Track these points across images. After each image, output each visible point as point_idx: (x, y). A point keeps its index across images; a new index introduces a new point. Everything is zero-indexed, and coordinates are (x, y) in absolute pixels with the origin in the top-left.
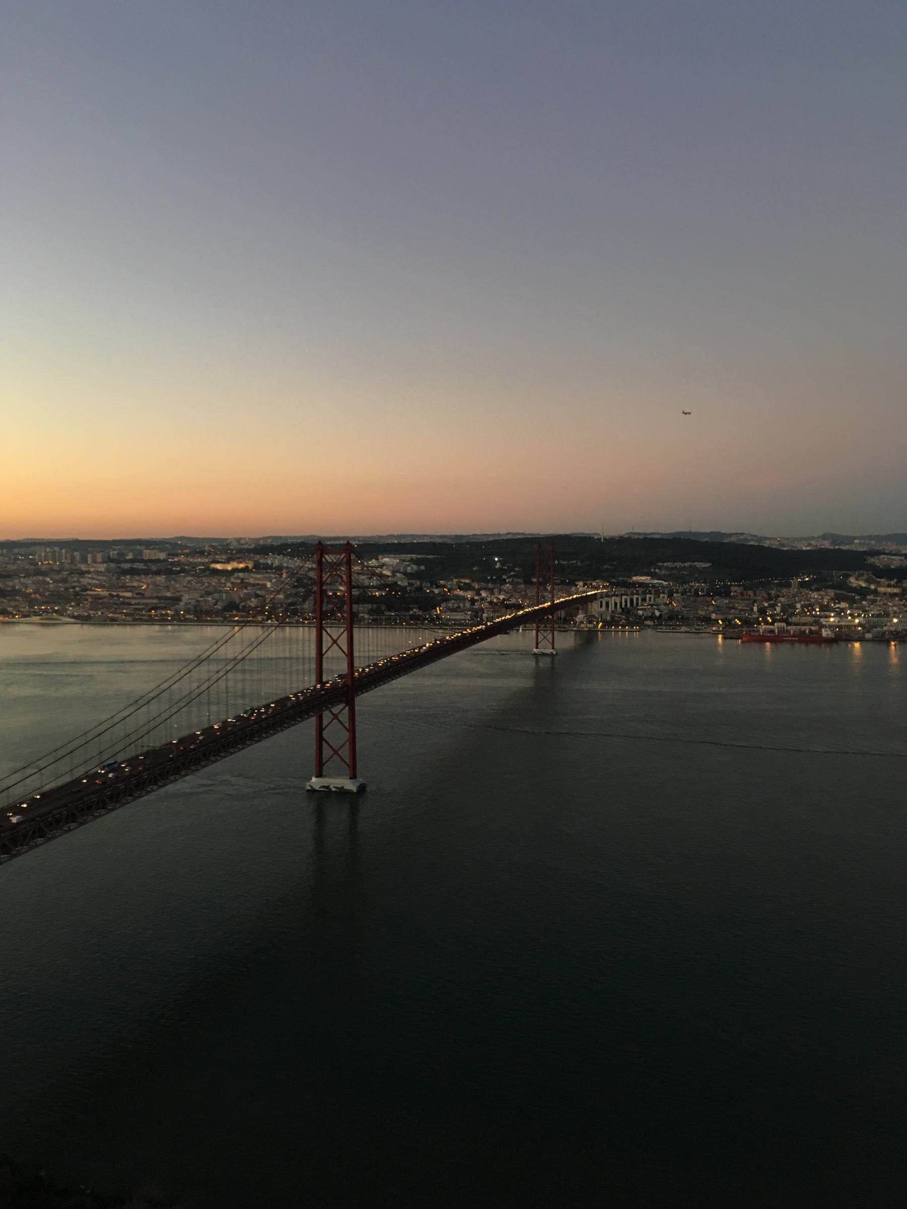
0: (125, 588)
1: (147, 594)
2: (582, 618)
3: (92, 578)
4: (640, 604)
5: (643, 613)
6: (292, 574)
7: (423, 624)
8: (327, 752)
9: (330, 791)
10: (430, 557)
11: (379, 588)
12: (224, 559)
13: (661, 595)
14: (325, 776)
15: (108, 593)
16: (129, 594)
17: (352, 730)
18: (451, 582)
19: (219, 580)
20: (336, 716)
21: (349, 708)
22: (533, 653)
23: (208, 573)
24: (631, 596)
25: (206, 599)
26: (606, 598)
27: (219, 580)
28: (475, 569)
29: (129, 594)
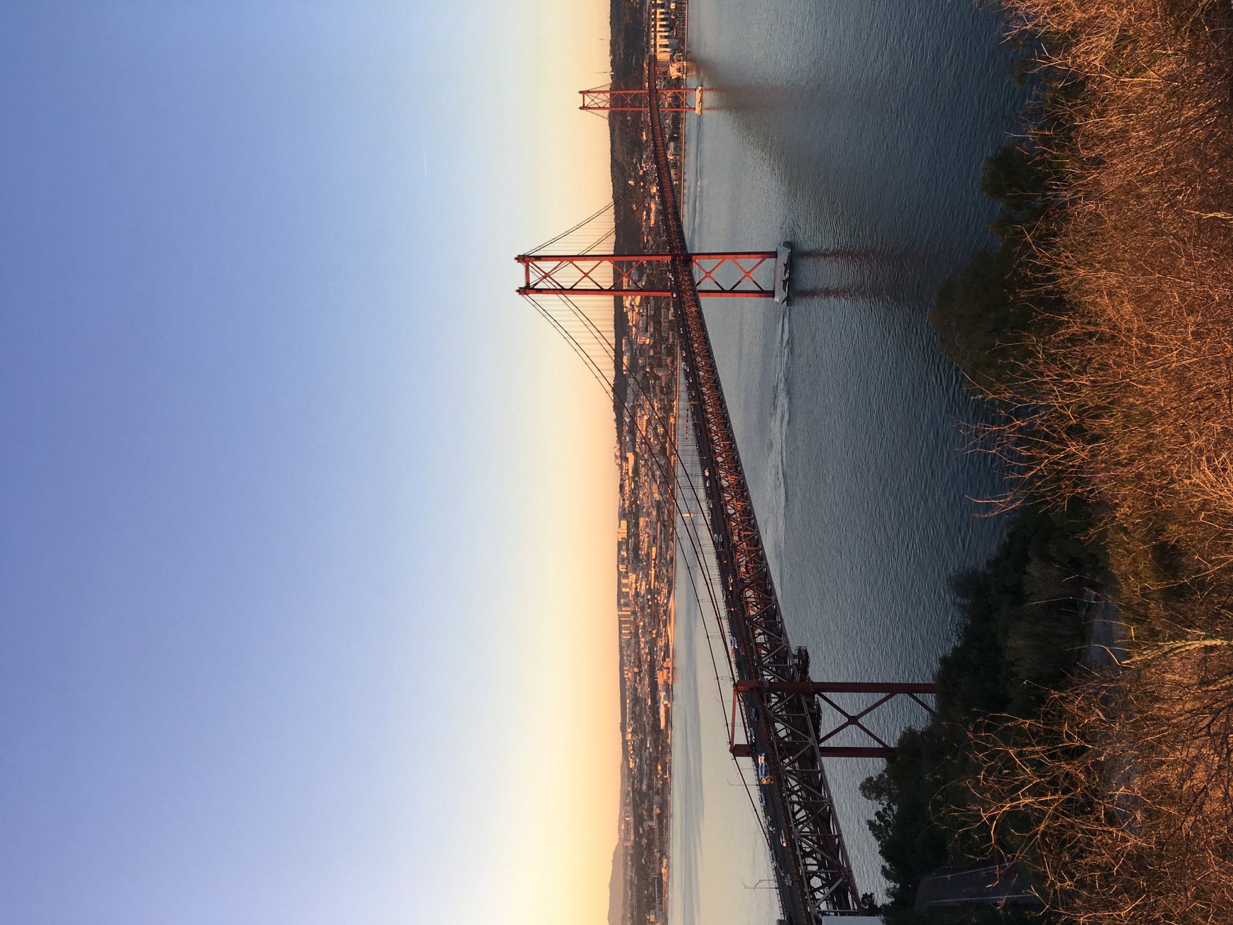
0: (648, 555)
1: (655, 534)
3: (641, 585)
6: (636, 397)
8: (747, 285)
9: (789, 279)
14: (774, 288)
15: (653, 569)
16: (654, 549)
19: (643, 466)
20: (708, 274)
23: (637, 479)
24: (657, 20)
25: (658, 476)
26: (658, 46)
27: (643, 466)
28: (635, 209)
29: (654, 549)
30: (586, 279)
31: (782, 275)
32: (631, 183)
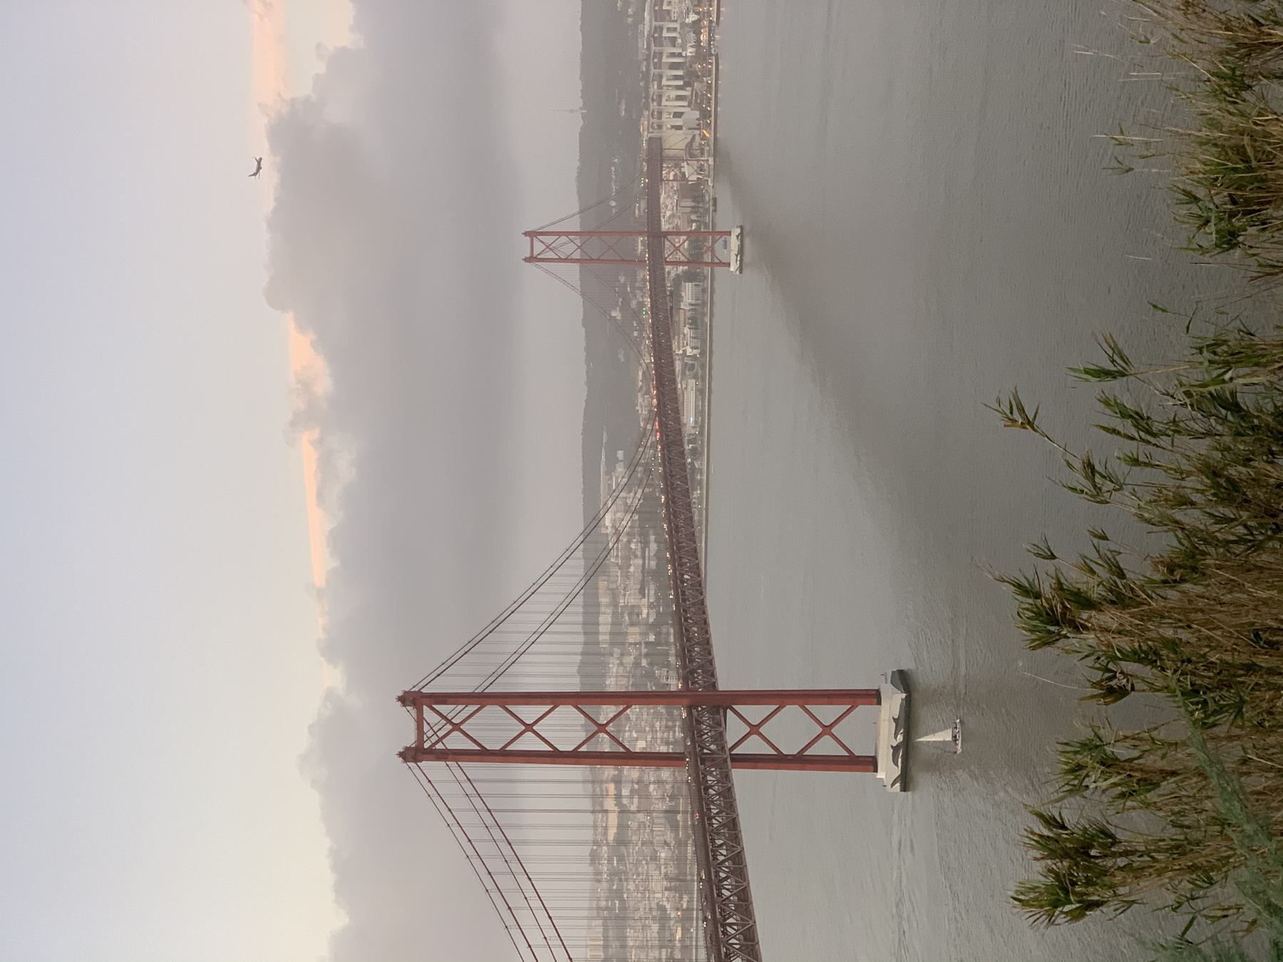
2: (690, 167)
4: (680, 51)
5: (691, 46)
7: (701, 471)
8: (826, 747)
10: (604, 441)
11: (645, 544)
12: (603, 817)
13: (665, 7)
14: (876, 752)
17: (781, 698)
18: (637, 408)
20: (755, 729)
21: (734, 704)
22: (738, 272)
26: (665, 116)
28: (623, 360)
30: (529, 734)
31: (886, 738)
32: (616, 314)
